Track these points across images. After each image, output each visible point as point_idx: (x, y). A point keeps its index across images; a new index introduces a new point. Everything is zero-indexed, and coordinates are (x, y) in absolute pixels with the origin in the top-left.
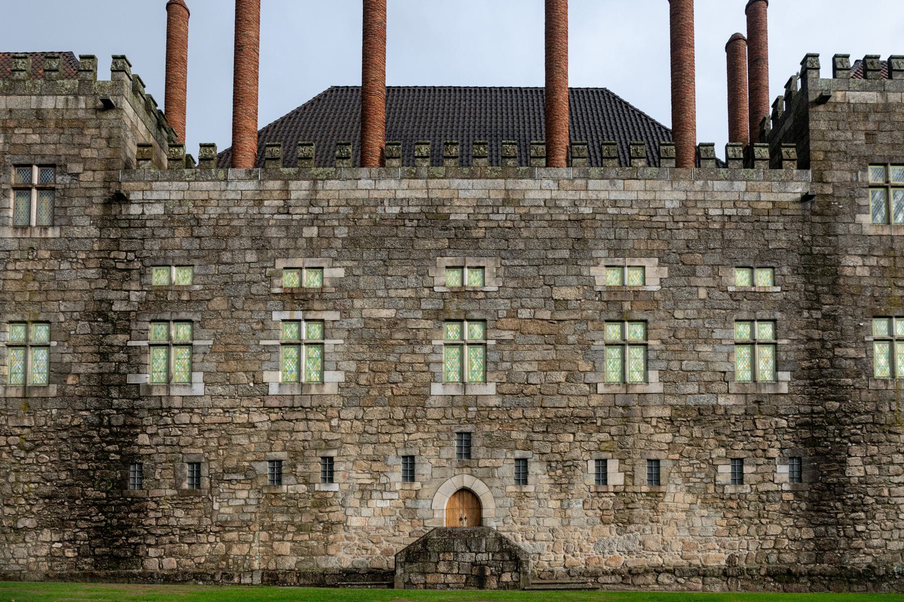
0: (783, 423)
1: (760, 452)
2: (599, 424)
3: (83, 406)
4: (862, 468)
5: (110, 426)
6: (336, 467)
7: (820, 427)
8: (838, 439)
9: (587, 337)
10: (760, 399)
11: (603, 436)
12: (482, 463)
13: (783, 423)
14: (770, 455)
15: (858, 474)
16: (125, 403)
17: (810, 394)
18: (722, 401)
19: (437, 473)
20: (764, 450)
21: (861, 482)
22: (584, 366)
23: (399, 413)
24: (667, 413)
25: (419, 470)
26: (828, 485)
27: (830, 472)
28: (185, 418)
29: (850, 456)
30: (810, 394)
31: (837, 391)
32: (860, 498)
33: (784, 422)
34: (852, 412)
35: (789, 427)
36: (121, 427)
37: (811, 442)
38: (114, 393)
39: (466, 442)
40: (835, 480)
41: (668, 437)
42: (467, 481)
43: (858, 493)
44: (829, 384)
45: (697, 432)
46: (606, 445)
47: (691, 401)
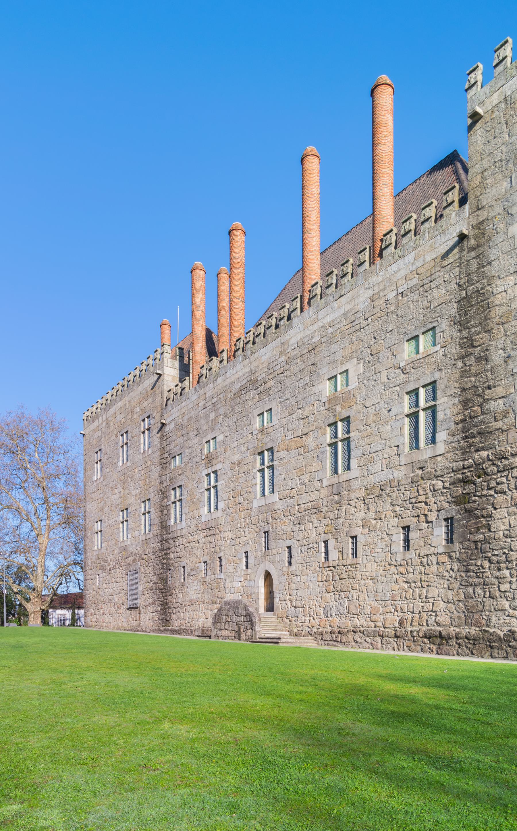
0: (439, 484)
1: (422, 517)
4: (506, 520)
8: (485, 492)
10: (422, 465)
13: (439, 484)
14: (429, 519)
15: (502, 527)
20: (426, 515)
21: (505, 536)
26: (475, 542)
27: (478, 529)
29: (495, 509)
32: (504, 553)
33: (440, 483)
35: (444, 488)
37: (458, 501)
40: (481, 537)
43: (502, 548)
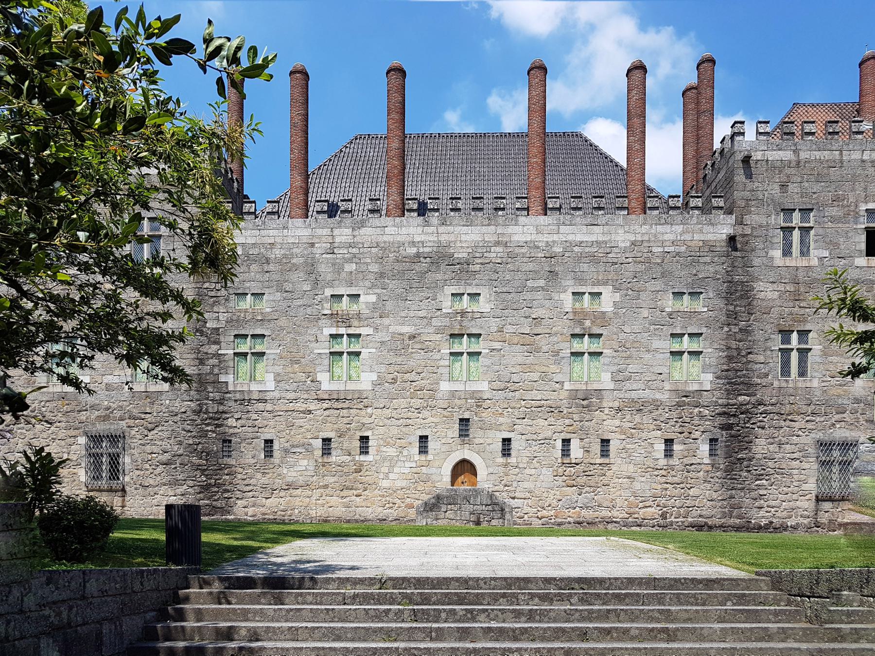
2: (565, 412)
3: (188, 398)
5: (207, 412)
6: (370, 444)
7: (734, 416)
9: (556, 347)
11: (567, 422)
12: (477, 441)
16: (217, 396)
17: (727, 390)
18: (658, 396)
19: (445, 448)
22: (553, 368)
23: (417, 403)
24: (616, 404)
25: (431, 445)
28: (261, 406)
30: (727, 390)
31: (749, 387)
34: (759, 405)
36: (216, 413)
38: (210, 389)
39: (464, 422)
41: (617, 422)
42: (468, 455)
44: (742, 383)
45: (637, 418)
46: (571, 428)
47: (634, 395)
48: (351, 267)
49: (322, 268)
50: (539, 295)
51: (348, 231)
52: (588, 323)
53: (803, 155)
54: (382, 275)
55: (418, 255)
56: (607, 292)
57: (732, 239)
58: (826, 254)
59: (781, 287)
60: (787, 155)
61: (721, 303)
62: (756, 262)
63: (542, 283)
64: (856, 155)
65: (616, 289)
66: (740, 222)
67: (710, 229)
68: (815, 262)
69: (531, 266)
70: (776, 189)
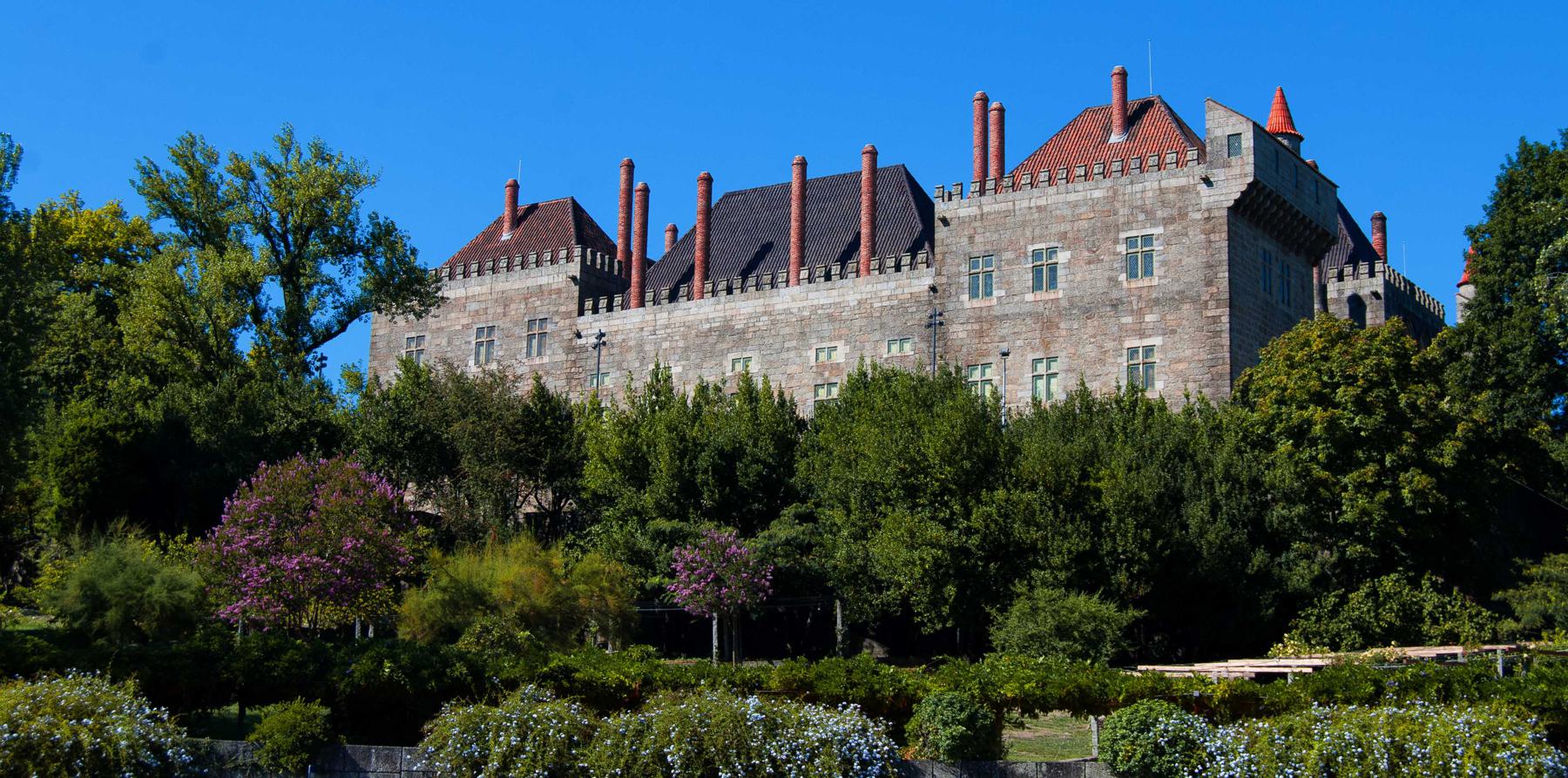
48: (666, 345)
49: (648, 348)
50: (792, 354)
51: (665, 315)
52: (827, 374)
53: (986, 209)
54: (686, 349)
55: (710, 330)
56: (840, 344)
57: (933, 289)
58: (1003, 293)
59: (969, 327)
60: (974, 211)
61: (923, 346)
62: (951, 306)
63: (794, 343)
64: (1025, 204)
65: (847, 342)
66: (938, 274)
67: (915, 282)
68: (994, 302)
69: (787, 330)
70: (965, 241)
